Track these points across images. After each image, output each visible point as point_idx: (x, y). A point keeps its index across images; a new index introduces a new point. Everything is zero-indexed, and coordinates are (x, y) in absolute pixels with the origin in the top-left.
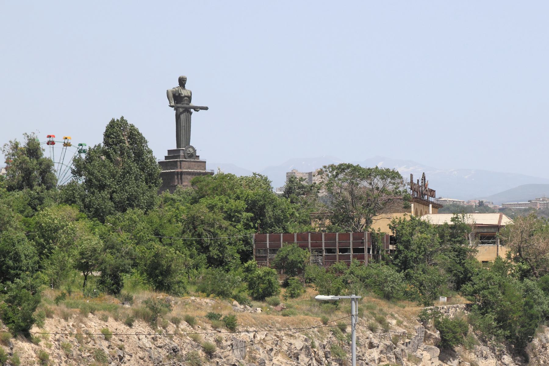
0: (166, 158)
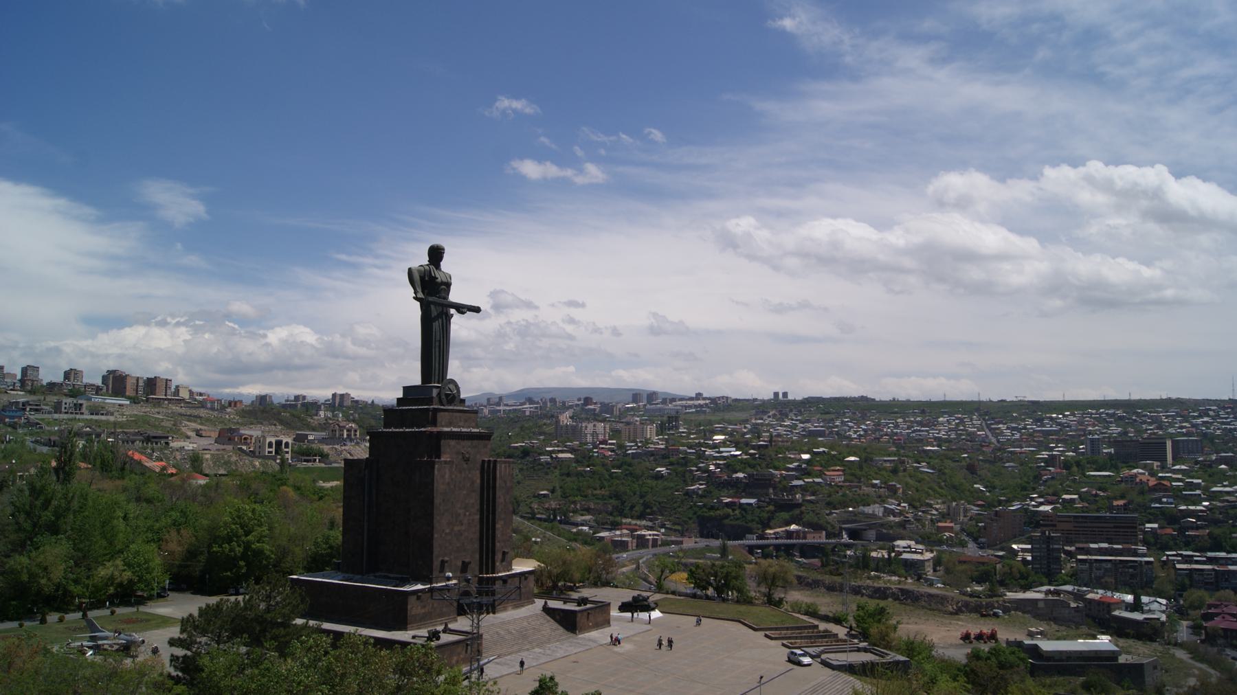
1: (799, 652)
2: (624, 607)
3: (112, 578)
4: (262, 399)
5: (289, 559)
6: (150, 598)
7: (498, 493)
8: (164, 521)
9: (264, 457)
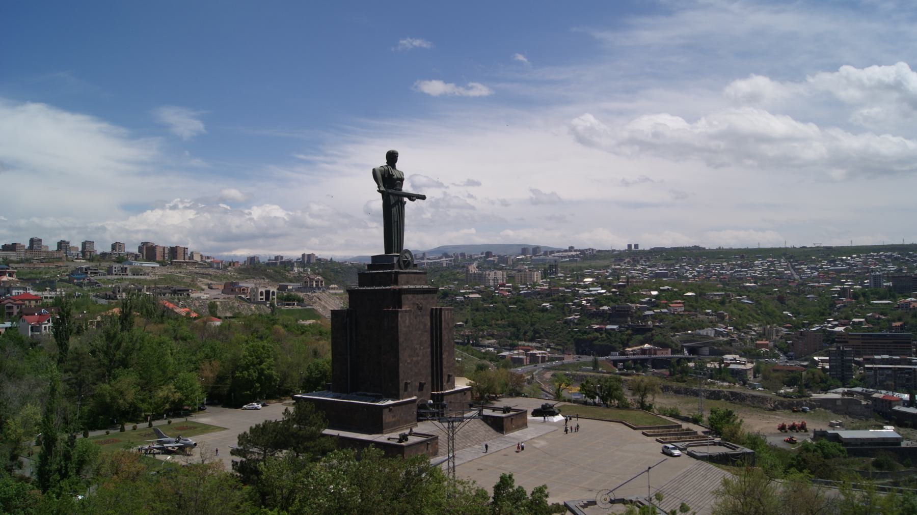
0: (370, 267)
1: (670, 446)
2: (536, 413)
3: (167, 398)
4: (252, 260)
5: (289, 380)
6: (194, 411)
7: (444, 332)
8: (200, 355)
9: (258, 303)
